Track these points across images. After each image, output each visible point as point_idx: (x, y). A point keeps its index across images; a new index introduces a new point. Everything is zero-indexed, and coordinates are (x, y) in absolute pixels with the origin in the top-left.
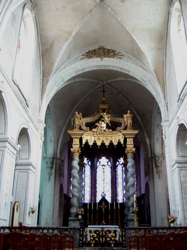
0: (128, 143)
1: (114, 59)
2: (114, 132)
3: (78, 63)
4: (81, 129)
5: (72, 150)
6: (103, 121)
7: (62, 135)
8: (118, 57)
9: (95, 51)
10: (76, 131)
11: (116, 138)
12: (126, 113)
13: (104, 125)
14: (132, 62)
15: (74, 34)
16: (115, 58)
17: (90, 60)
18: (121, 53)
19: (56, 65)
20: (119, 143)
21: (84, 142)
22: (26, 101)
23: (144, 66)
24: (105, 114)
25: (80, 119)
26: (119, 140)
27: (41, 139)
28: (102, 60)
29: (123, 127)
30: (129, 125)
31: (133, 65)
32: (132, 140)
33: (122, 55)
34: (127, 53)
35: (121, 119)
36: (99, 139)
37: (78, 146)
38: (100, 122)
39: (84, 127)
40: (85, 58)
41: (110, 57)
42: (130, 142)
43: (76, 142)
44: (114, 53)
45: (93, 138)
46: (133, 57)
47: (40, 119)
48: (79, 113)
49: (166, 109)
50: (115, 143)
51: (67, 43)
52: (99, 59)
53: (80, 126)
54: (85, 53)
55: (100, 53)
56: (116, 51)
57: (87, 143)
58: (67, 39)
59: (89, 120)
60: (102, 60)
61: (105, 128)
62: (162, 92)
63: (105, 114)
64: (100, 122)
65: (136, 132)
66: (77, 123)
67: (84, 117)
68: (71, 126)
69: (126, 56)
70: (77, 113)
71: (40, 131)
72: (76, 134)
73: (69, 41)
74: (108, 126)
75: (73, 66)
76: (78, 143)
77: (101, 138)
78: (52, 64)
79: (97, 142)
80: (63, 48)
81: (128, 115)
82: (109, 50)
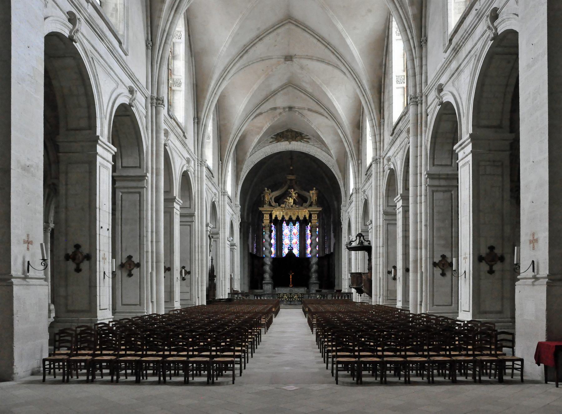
0: (313, 219)
1: (302, 143)
2: (301, 208)
3: (267, 147)
4: (270, 205)
5: (263, 224)
6: (291, 197)
7: (248, 198)
8: (305, 141)
9: (282, 133)
10: (266, 208)
11: (303, 213)
12: (312, 190)
13: (291, 201)
14: (318, 146)
15: (264, 129)
16: (302, 142)
17: (278, 143)
18: (308, 136)
19: (248, 154)
20: (305, 218)
21: (273, 218)
22: (231, 200)
23: (328, 152)
24: (292, 190)
25: (270, 194)
26: (305, 216)
27: (239, 221)
28: (290, 143)
29: (308, 203)
30: (314, 201)
31: (319, 150)
32: (316, 215)
33: (309, 139)
34: (314, 137)
35: (308, 194)
36: (287, 214)
37: (269, 221)
38: (288, 198)
39: (273, 204)
40: (274, 141)
41: (297, 141)
42: (315, 217)
43: (266, 217)
44: (302, 137)
45: (282, 213)
46: (319, 141)
47: (237, 204)
48: (268, 190)
49: (345, 196)
50: (301, 218)
51: (259, 137)
52: (287, 142)
53: (270, 202)
54: (274, 135)
55: (288, 135)
56: (303, 134)
57: (276, 218)
58: (258, 133)
59: (276, 193)
60: (290, 143)
61: (292, 204)
62: (343, 180)
63: (292, 190)
64: (288, 198)
65: (320, 209)
66: (266, 199)
67: (272, 192)
68: (260, 202)
69: (312, 139)
70: (266, 189)
71: (237, 214)
72: (266, 211)
73: (261, 135)
74: (295, 202)
75: (263, 150)
76: (268, 218)
77: (289, 213)
78: (246, 154)
79: (285, 216)
80: (255, 140)
81: (313, 191)
82: (297, 132)
